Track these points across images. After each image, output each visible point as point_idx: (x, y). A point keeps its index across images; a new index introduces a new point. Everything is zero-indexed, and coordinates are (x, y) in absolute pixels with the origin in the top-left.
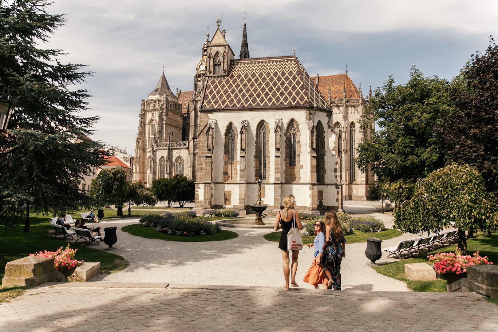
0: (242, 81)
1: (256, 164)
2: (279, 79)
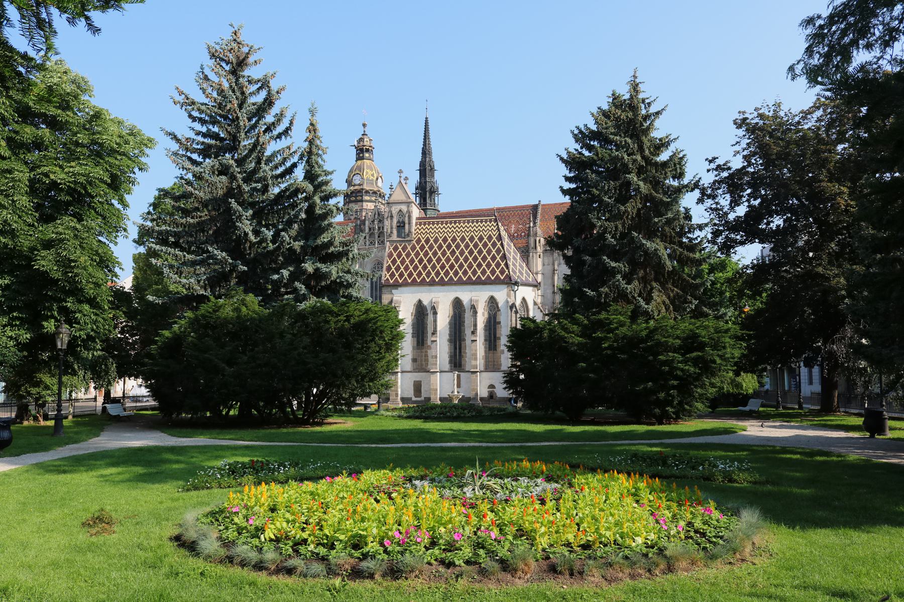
0: (431, 247)
1: (450, 349)
2: (476, 246)
